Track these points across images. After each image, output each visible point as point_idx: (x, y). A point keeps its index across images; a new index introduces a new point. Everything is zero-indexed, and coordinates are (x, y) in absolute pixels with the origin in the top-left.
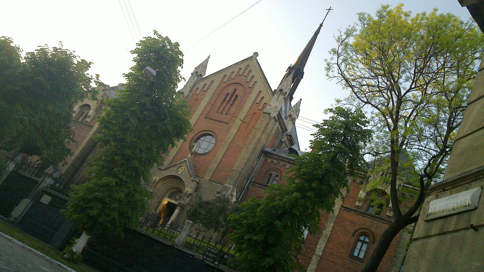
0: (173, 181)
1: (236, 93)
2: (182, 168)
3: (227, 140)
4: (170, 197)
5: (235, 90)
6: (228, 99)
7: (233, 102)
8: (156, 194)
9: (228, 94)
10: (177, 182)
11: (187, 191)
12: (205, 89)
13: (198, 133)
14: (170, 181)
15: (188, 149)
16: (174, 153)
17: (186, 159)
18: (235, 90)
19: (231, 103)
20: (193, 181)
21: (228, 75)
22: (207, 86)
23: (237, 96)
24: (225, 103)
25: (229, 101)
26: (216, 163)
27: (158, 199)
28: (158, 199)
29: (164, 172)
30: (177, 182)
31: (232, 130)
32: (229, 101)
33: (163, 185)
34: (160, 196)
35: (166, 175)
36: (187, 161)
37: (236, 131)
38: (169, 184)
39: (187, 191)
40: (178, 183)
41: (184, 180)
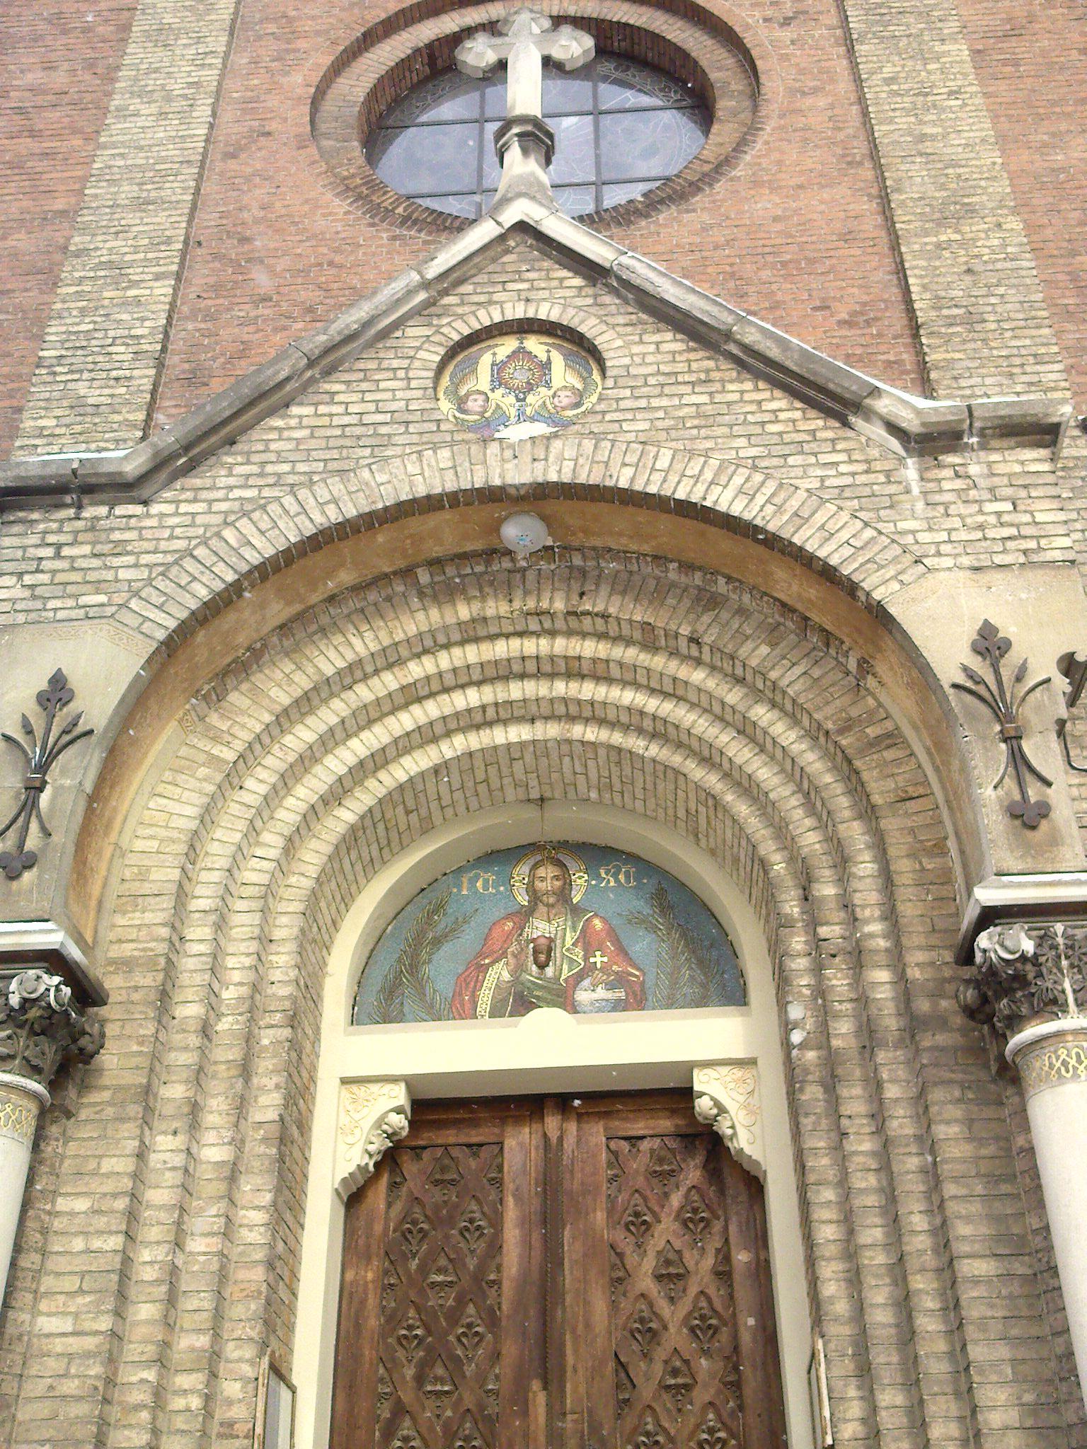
0: (390, 659)
2: (521, 352)
4: (391, 993)
8: (164, 998)
10: (501, 649)
13: (369, 39)
14: (354, 673)
15: (340, 206)
20: (933, 442)
26: (971, 211)
27: (241, 1106)
28: (241, 1106)
29: (171, 511)
30: (501, 649)
33: (232, 777)
34: (253, 1008)
35: (265, 548)
38: (329, 741)
41: (725, 500)
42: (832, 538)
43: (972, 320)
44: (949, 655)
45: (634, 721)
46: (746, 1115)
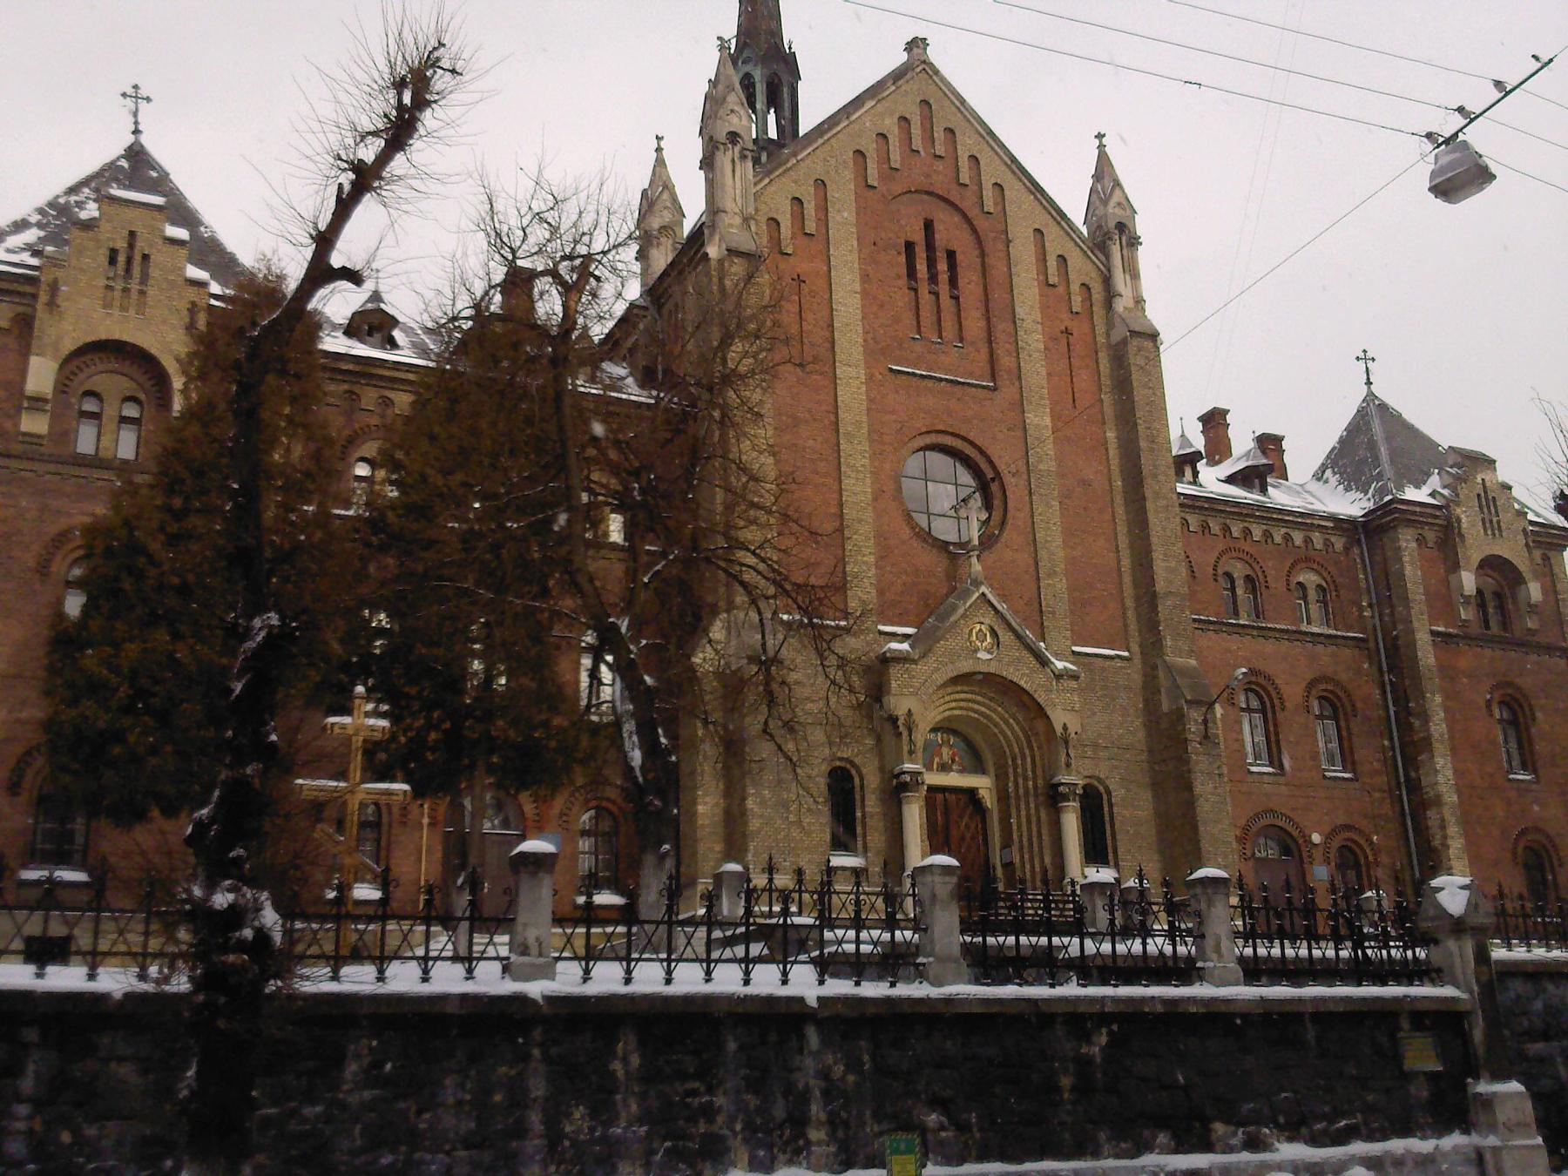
1: (940, 238)
3: (1041, 467)
5: (929, 226)
6: (922, 267)
7: (953, 281)
9: (909, 246)
11: (1065, 728)
12: (811, 226)
16: (865, 563)
17: (983, 589)
18: (929, 226)
19: (944, 288)
21: (871, 149)
22: (810, 208)
23: (951, 255)
24: (924, 289)
25: (933, 278)
31: (1030, 417)
32: (933, 278)
36: (990, 597)
37: (1048, 421)
39: (1065, 728)
40: (979, 698)
41: (1022, 683)
42: (1041, 697)
43: (1054, 613)
44: (1059, 730)
45: (982, 714)
46: (988, 798)
